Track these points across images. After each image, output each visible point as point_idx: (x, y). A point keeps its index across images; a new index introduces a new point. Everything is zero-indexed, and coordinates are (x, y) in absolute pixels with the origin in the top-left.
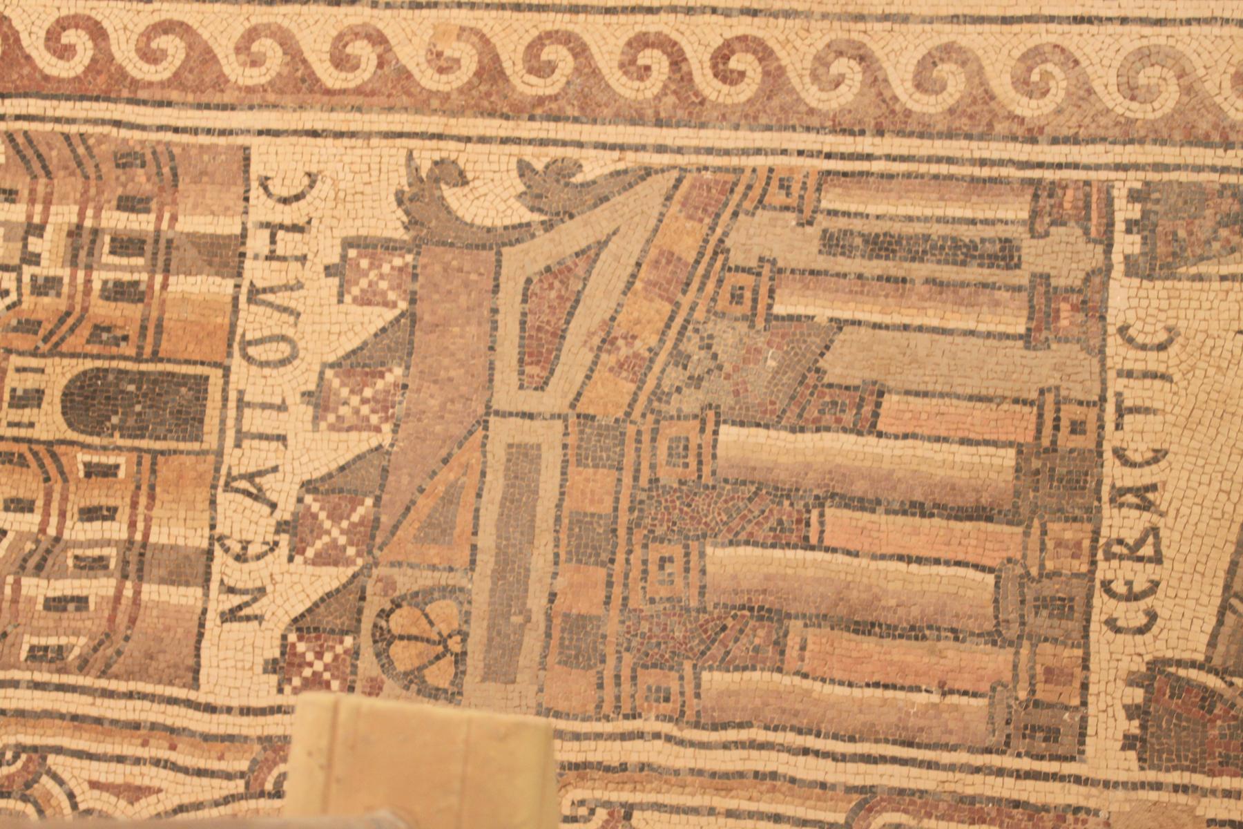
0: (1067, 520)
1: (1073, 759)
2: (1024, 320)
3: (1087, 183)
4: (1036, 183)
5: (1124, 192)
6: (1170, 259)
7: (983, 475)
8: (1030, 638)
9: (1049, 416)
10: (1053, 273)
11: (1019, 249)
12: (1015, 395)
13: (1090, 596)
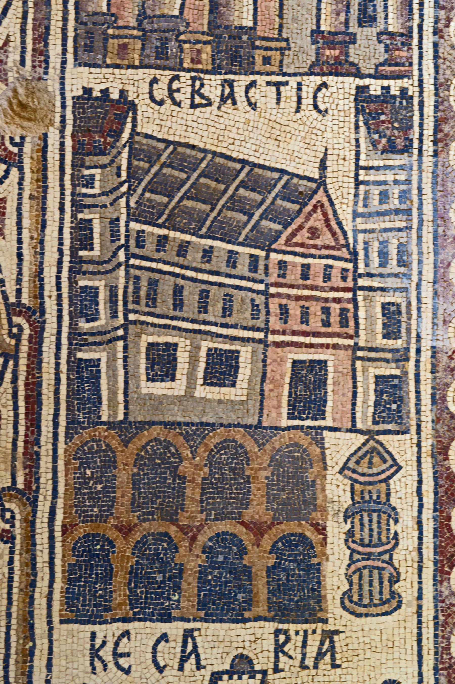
0: (213, 55)
1: (76, 60)
2: (328, 29)
3: (411, 64)
4: (409, 35)
5: (406, 85)
6: (367, 111)
7: (237, 7)
8: (144, 35)
9: (273, 44)
10: (357, 45)
11: (371, 26)
12: (285, 25)
13: (170, 69)
